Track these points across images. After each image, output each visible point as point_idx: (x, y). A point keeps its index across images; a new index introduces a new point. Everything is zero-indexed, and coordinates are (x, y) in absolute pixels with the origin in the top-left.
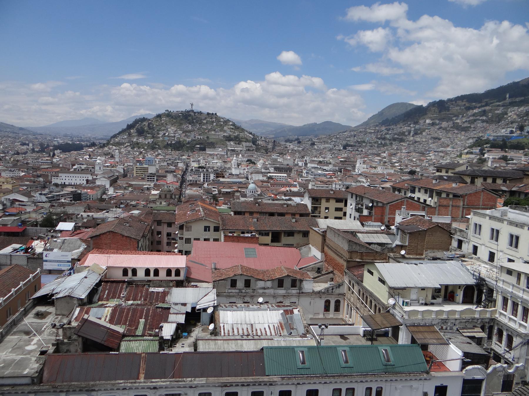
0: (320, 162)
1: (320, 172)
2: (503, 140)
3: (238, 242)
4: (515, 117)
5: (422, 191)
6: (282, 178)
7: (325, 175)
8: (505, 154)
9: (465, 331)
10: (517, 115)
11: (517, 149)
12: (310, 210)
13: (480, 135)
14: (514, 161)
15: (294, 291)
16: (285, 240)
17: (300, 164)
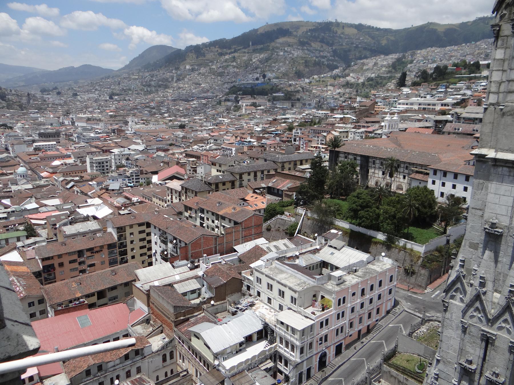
0: (89, 119)
1: (92, 135)
2: (252, 87)
3: (69, 312)
4: (258, 63)
5: (210, 213)
6: (50, 146)
7: (98, 139)
8: (254, 101)
9: (262, 365)
10: (260, 62)
11: (262, 95)
12: (116, 238)
13: (233, 79)
14: (262, 107)
15: (138, 358)
16: (110, 295)
17: (66, 122)
